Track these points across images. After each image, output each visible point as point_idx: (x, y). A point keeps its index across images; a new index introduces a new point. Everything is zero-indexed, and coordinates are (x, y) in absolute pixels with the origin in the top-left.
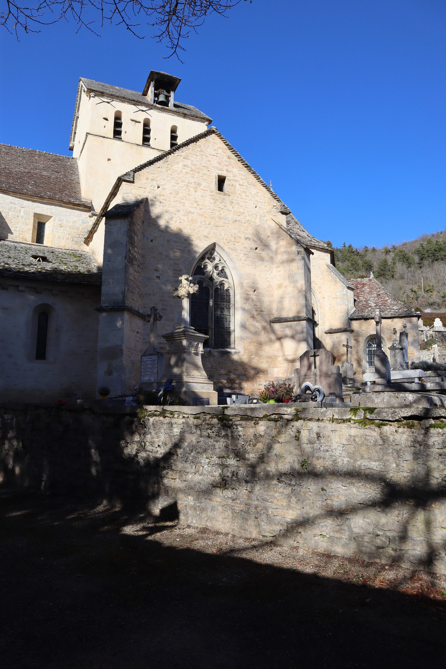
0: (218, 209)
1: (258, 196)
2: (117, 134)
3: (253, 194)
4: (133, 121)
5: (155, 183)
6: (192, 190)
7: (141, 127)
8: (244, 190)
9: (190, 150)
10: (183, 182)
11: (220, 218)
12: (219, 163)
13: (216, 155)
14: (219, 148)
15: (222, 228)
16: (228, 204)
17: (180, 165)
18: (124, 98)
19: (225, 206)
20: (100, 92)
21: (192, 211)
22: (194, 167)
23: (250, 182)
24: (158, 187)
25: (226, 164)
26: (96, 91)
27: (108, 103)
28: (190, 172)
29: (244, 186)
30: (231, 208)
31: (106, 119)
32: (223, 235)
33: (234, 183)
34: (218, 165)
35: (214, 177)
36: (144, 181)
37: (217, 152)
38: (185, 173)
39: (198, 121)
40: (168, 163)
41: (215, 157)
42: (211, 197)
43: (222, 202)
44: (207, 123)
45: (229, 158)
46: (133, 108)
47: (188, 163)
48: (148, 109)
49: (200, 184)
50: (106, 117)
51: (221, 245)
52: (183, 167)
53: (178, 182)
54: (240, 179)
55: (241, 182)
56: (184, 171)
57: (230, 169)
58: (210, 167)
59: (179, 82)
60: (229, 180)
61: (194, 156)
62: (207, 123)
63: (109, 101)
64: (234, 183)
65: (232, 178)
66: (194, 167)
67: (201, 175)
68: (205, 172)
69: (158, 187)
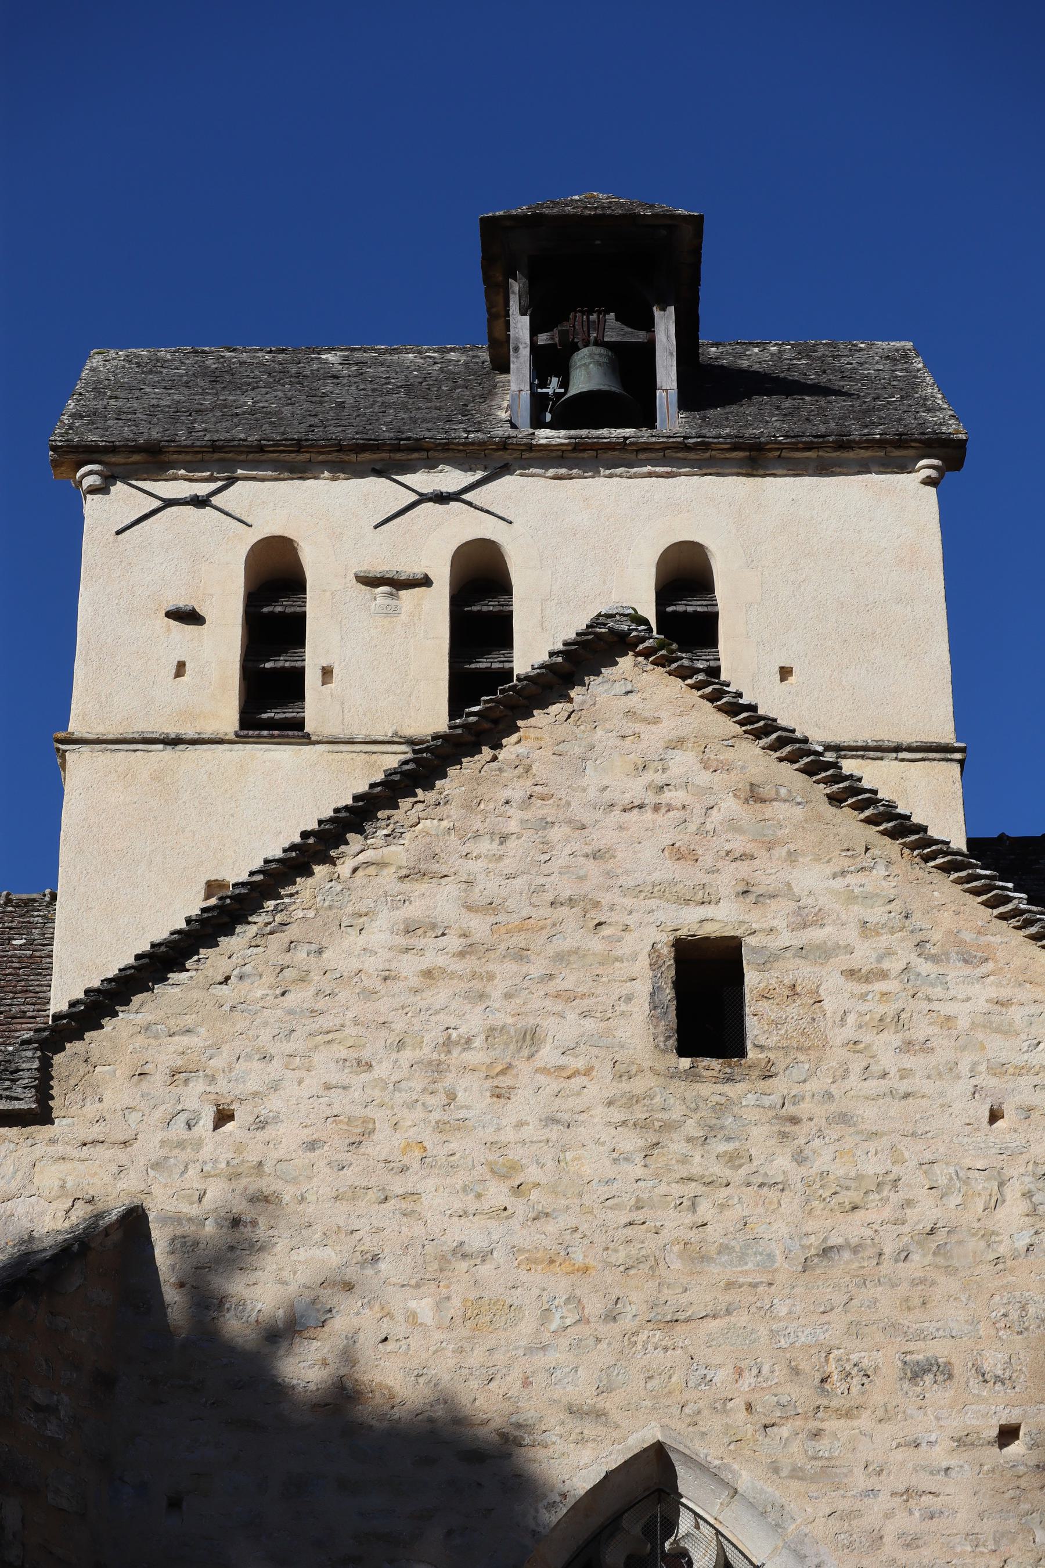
0: (677, 1190)
1: (1007, 1031)
2: (272, 696)
3: (963, 1023)
4: (371, 581)
6: (473, 1095)
7: (431, 614)
8: (890, 1009)
9: (454, 811)
10: (401, 1044)
12: (678, 853)
13: (650, 799)
14: (677, 744)
15: (713, 1325)
16: (759, 1138)
17: (380, 932)
18: (299, 446)
19: (732, 1160)
20: (137, 449)
21: (477, 1242)
22: (479, 926)
23: (936, 936)
24: (223, 1117)
25: (738, 844)
26: (112, 449)
27: (200, 502)
28: (458, 966)
29: (884, 975)
30: (782, 1164)
31: (189, 617)
32: (721, 1376)
33: (803, 972)
34: (668, 870)
35: (642, 966)
36: (116, 1091)
37: (660, 779)
38: (415, 981)
39: (864, 469)
40: (293, 932)
41: (648, 815)
42: (617, 1115)
44: (926, 467)
45: (754, 795)
46: (380, 493)
47: (440, 901)
48: (479, 475)
50: (183, 602)
51: (710, 1452)
52: (402, 941)
53: (365, 1054)
54: (851, 935)
55: (864, 955)
56: (409, 966)
57: (768, 872)
58: (606, 898)
59: (699, 234)
60: (768, 960)
61: (486, 846)
62: (926, 467)
63: (203, 489)
64: (803, 972)
65: (785, 938)
66: (479, 926)
67: (536, 969)
68: (573, 936)
69: (223, 1117)
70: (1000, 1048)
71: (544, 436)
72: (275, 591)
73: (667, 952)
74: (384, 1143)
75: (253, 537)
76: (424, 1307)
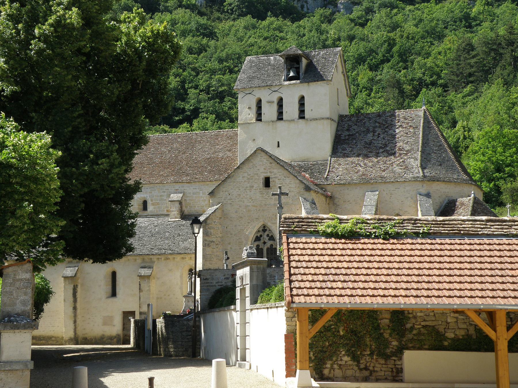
5: (227, 193)
11: (266, 205)
17: (241, 178)
22: (249, 177)
33: (274, 179)
43: (267, 194)
47: (246, 175)
49: (253, 187)
55: (279, 178)
56: (243, 180)
57: (272, 170)
60: (272, 178)
64: (274, 179)
66: (249, 177)
68: (256, 177)
70: (290, 185)
71: (287, 83)
72: (259, 103)
73: (264, 179)
74: (242, 196)
75: (256, 97)
76: (245, 210)
